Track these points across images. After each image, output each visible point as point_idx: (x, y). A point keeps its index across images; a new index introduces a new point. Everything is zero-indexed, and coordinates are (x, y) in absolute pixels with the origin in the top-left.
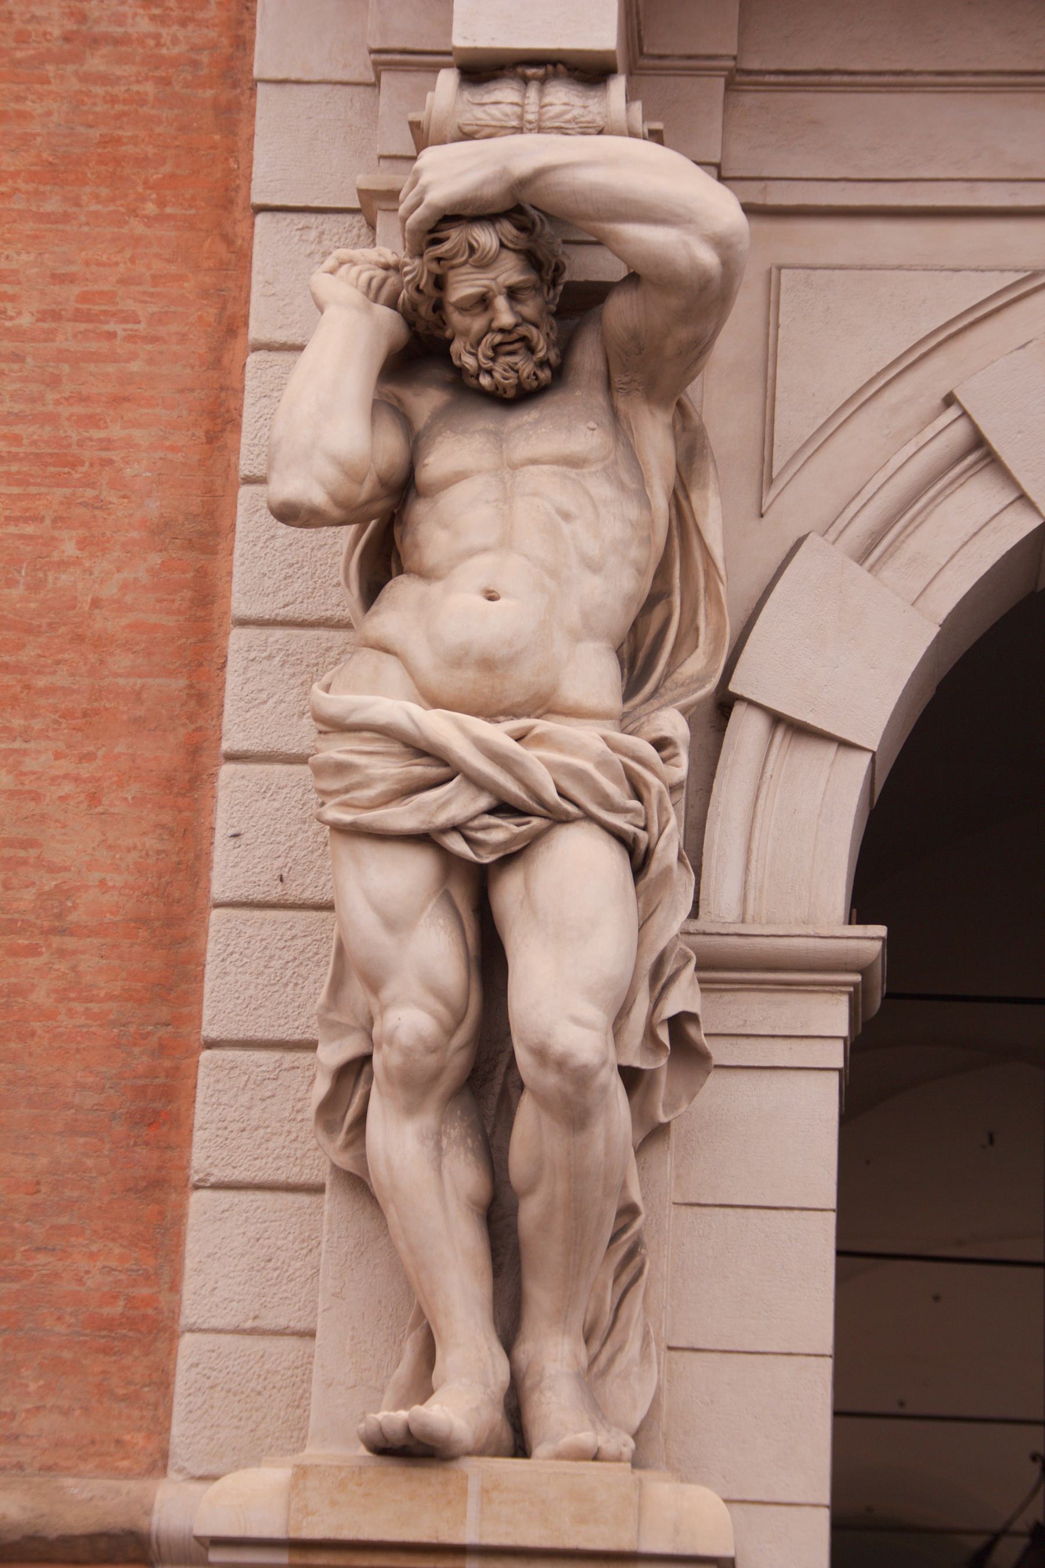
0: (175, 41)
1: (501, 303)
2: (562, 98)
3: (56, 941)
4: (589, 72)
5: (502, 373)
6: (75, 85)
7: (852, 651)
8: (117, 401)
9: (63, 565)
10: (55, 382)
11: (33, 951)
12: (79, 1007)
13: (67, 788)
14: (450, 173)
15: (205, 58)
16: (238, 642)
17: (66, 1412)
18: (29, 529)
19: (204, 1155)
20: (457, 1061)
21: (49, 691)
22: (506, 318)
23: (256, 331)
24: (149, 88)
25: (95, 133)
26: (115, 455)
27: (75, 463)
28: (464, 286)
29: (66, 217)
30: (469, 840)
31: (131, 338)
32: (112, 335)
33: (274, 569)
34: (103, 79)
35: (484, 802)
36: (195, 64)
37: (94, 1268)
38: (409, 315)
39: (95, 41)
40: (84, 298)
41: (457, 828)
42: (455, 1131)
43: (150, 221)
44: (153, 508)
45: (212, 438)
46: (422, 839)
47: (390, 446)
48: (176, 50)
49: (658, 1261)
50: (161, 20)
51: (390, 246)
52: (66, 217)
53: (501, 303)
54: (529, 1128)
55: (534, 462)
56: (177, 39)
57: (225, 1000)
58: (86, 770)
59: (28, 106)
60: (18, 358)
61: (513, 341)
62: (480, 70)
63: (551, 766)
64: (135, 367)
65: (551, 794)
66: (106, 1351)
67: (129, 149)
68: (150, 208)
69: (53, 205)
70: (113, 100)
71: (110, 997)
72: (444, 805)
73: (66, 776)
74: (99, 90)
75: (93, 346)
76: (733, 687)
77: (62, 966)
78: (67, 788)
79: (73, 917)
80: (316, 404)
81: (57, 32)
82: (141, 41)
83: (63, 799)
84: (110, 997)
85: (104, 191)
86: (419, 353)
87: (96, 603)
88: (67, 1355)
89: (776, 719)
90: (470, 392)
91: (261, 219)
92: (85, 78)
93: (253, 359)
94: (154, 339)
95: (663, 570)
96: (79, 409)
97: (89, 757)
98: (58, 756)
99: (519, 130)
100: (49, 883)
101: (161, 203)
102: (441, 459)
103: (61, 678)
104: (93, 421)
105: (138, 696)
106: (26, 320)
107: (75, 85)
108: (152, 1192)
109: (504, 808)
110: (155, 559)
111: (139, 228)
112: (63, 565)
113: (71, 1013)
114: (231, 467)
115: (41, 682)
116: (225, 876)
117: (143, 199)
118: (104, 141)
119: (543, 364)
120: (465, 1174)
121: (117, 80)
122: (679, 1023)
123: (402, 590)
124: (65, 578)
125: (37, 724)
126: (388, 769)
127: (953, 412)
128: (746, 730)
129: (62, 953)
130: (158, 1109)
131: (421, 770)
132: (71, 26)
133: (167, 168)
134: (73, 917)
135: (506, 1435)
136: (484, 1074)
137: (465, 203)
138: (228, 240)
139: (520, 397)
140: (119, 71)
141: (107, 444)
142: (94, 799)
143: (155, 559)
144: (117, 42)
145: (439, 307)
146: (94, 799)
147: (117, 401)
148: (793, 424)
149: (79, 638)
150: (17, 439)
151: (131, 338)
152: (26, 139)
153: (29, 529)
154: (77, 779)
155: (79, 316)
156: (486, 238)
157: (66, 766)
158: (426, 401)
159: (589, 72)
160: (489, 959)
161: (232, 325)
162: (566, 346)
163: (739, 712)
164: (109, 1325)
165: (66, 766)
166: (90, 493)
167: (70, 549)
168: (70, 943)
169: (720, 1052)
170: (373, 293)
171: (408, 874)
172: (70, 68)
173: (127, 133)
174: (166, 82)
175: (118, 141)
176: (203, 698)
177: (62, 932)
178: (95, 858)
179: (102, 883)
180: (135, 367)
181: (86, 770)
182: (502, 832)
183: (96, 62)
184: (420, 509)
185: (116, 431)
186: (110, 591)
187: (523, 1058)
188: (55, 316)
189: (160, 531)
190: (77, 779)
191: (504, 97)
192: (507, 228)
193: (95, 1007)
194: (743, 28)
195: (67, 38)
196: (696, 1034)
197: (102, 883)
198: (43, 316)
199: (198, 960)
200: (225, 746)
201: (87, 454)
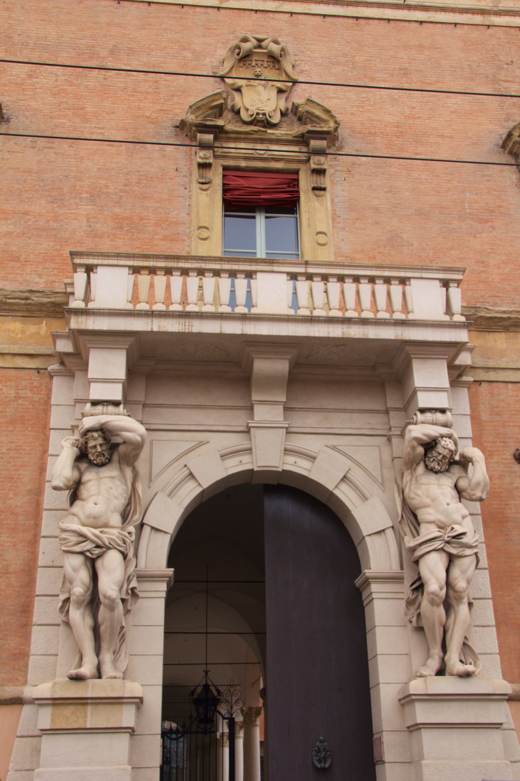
0: (36, 397)
1: (98, 447)
2: (111, 408)
3: (6, 575)
4: (116, 404)
5: (98, 460)
6: (16, 406)
7: (167, 514)
8: (22, 466)
9: (10, 499)
10: (9, 462)
12: (10, 589)
13: (9, 544)
14: (89, 422)
15: (42, 401)
16: (45, 514)
17: (6, 673)
18: (3, 492)
19: (36, 618)
20: (88, 598)
21: (5, 524)
22: (99, 449)
23: (50, 452)
24: (31, 406)
25: (20, 415)
26: (21, 477)
27: (13, 478)
28: (91, 444)
29: (13, 431)
30: (91, 553)
31: (25, 454)
32: (21, 453)
33: (52, 499)
34: (22, 405)
35: (94, 545)
36: (40, 402)
37: (13, 643)
38: (80, 449)
39: (20, 398)
40: (16, 446)
41: (88, 551)
42: (87, 612)
43: (30, 431)
44: (29, 487)
45: (41, 473)
46: (81, 553)
47: (76, 474)
48: (36, 399)
49: (128, 638)
50: (34, 394)
51: (77, 436)
52: (13, 431)
53: (98, 447)
54: (102, 611)
55: (105, 477)
56: (36, 397)
57: (40, 587)
58: (13, 540)
59: (7, 410)
60: (2, 458)
61: (101, 454)
62: (95, 403)
63: (108, 538)
64: (26, 459)
65: (107, 544)
66: (15, 660)
67: (26, 418)
68: (30, 429)
69: (11, 428)
70: (23, 409)
71: (17, 587)
72: (86, 546)
73: (9, 541)
74: (21, 407)
75: (17, 455)
76: (144, 521)
77: (7, 580)
78: (9, 544)
79: (10, 570)
80: (61, 466)
81: (13, 396)
82: (29, 397)
83: (8, 546)
84: (17, 587)
85: (21, 426)
86: (82, 456)
87: (16, 506)
88: (6, 661)
89: (153, 528)
90: (92, 464)
91: (52, 431)
92: (18, 404)
93: (49, 458)
94: (29, 454)
95: (130, 499)
96: (14, 468)
97: (14, 537)
98: (8, 537)
99: (102, 414)
100: (5, 563)
101: (32, 428)
102: (87, 477)
103: (9, 522)
104: (17, 470)
105: (24, 525)
106: (4, 451)
107: (16, 406)
108: (25, 627)
109: (98, 546)
110: (28, 497)
111: (27, 432)
112: (10, 499)
113: (9, 590)
114: (44, 479)
115: (5, 522)
116: (42, 561)
117: (28, 427)
118: (21, 416)
119: (107, 459)
120: (89, 621)
121: (24, 405)
122: (133, 589)
123: (78, 503)
124: (10, 501)
126: (74, 539)
127: (186, 468)
128: (146, 530)
129: (7, 578)
130: (26, 610)
131: (81, 539)
132: (16, 395)
133: (34, 421)
134: (10, 570)
135: (97, 674)
136: (93, 601)
137: (92, 428)
138: (45, 435)
139: (102, 465)
140: (25, 403)
141: (19, 475)
142: (15, 546)
143: (28, 497)
144: (24, 398)
145: (86, 448)
146: (15, 546)
147: (22, 466)
148: (155, 470)
149: (12, 513)
151: (25, 454)
152: (6, 416)
153: (3, 492)
154: (11, 542)
155: (15, 450)
156: (96, 435)
157: (10, 539)
158: (83, 466)
159: (116, 404)
160: (94, 577)
161: (45, 451)
162: (111, 455)
163: (145, 526)
164: (15, 654)
165: (10, 539)
166: (16, 484)
167: (11, 495)
168: (9, 575)
169: (141, 595)
170: (73, 445)
171: (78, 560)
172: (15, 403)
173: (26, 415)
174: (34, 405)
175: (24, 416)
176: (37, 525)
177: (7, 573)
178: (15, 558)
179: (16, 563)
180: (26, 459)
181: (13, 540)
182: (97, 551)
183: (20, 402)
184: (82, 487)
185: (21, 472)
186: (19, 504)
187: (101, 597)
188: (10, 450)
189: (30, 491)
190: (11, 542)
191: (99, 408)
192: (100, 433)
193: (14, 589)
194: (146, 396)
195: (15, 397)
196: (136, 591)
197: (16, 563)
198: (8, 450)
199: (35, 578)
200: (42, 535)
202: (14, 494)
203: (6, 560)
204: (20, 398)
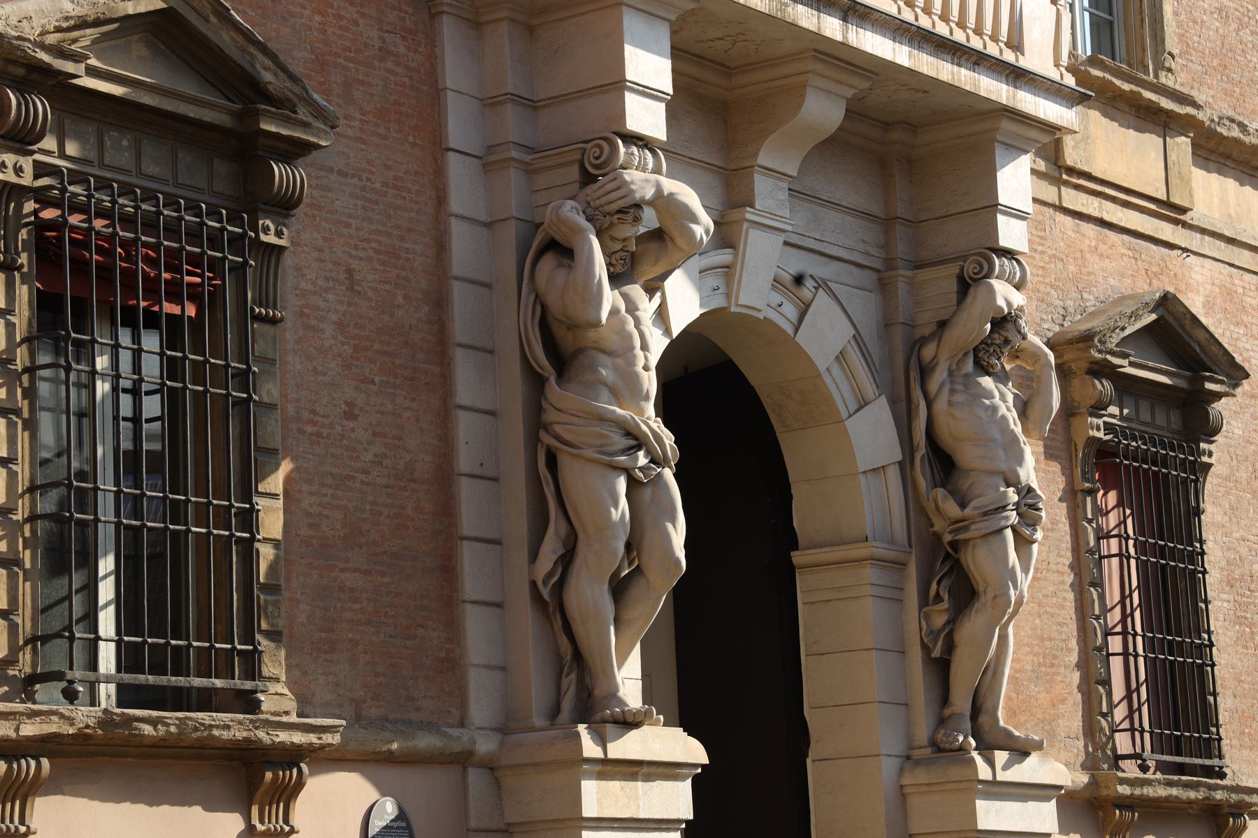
8: (410, 230)
9: (399, 306)
11: (405, 489)
24: (406, 80)
25: (393, 98)
27: (399, 258)
58: (414, 405)
60: (377, 203)
68: (411, 139)
69: (382, 131)
75: (400, 202)
87: (410, 326)
92: (387, 70)
97: (413, 400)
106: (378, 185)
124: (400, 313)
125: (398, 382)
141: (408, 251)
147: (410, 230)
150: (380, 243)
152: (372, 95)
155: (395, 187)
167: (400, 300)
180: (413, 215)
201: (403, 254)
202: (405, 297)
203: (409, 452)
204: (389, 53)
